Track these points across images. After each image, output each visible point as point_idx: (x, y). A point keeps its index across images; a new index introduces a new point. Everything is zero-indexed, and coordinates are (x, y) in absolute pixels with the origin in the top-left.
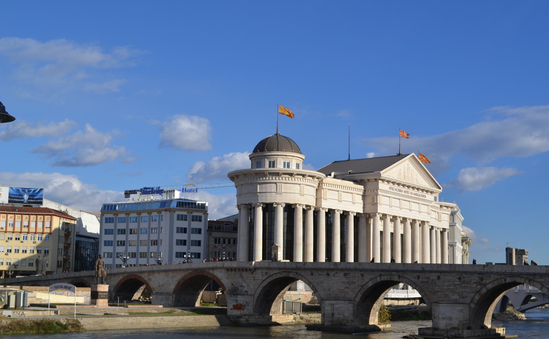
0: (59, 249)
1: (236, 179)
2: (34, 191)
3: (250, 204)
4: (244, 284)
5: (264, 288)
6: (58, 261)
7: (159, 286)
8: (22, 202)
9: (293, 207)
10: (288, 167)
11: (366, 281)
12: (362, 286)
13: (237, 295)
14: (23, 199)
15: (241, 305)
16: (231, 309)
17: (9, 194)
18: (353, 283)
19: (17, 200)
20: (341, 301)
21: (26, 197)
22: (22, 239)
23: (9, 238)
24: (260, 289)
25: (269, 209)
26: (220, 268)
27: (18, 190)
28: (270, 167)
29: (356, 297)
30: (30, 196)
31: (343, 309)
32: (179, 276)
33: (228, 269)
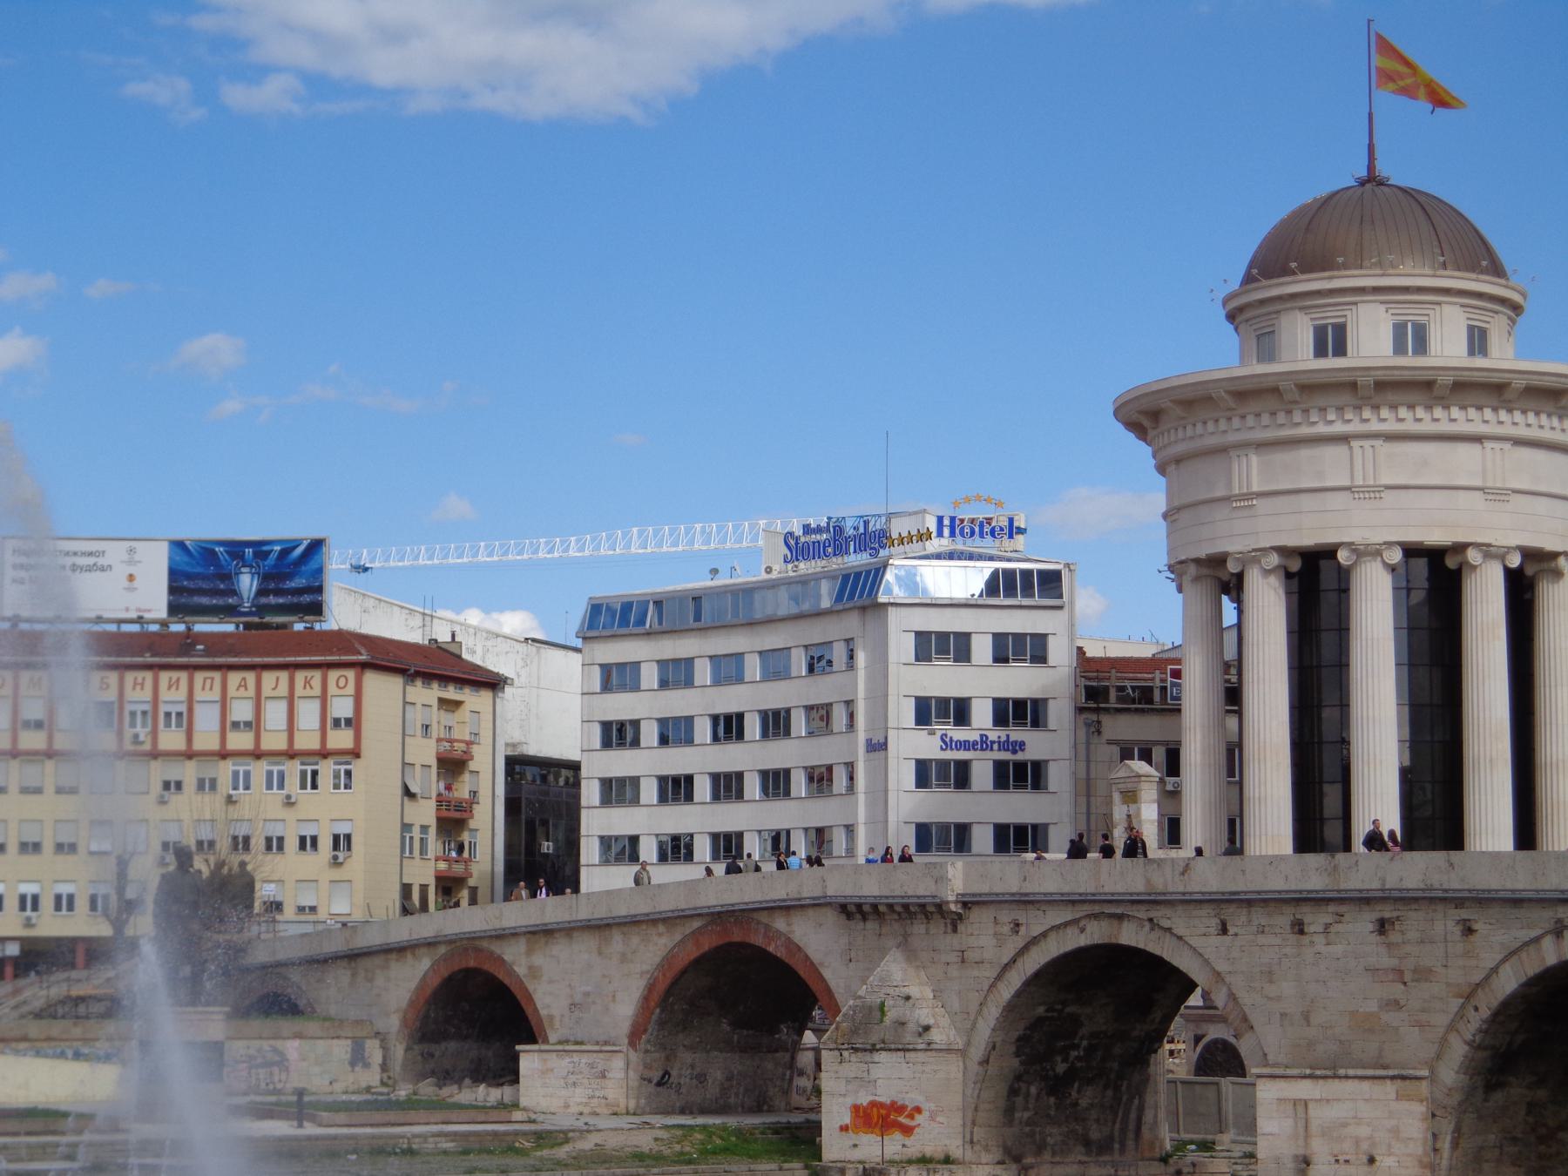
0: (406, 827)
1: (1151, 433)
2: (285, 552)
3: (1219, 561)
4: (914, 991)
5: (1010, 1008)
6: (406, 889)
7: (573, 1006)
8: (230, 611)
9: (1451, 563)
10: (1421, 346)
11: (1489, 959)
12: (1470, 995)
13: (873, 1049)
14: (234, 592)
15: (899, 1109)
16: (844, 1129)
17: (173, 574)
18: (1422, 974)
19: (205, 601)
20: (1350, 1085)
21: (247, 583)
22: (224, 785)
23: (167, 785)
24: (993, 1012)
25: (1316, 582)
26: (818, 904)
27: (207, 552)
28: (1320, 351)
29: (1439, 1057)
30: (266, 578)
31: (1363, 1131)
32: (649, 955)
33: (853, 911)
